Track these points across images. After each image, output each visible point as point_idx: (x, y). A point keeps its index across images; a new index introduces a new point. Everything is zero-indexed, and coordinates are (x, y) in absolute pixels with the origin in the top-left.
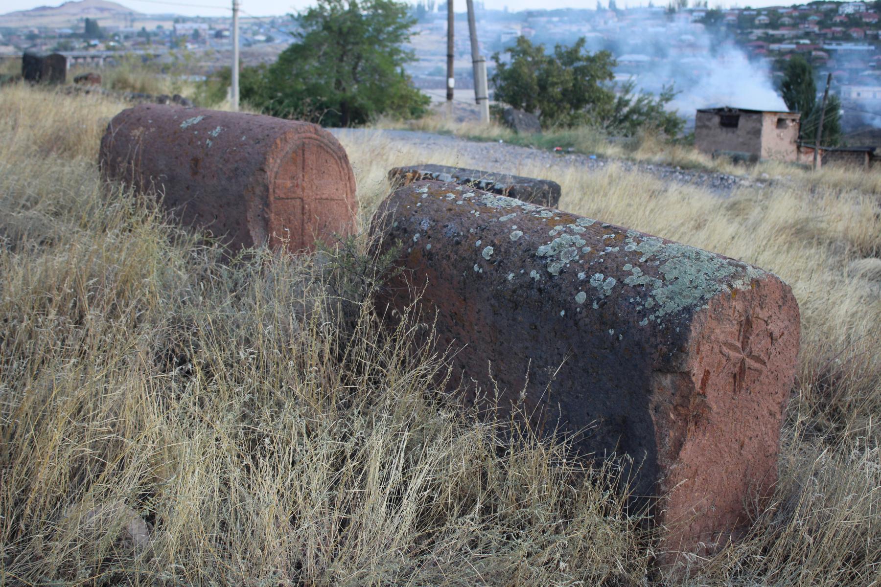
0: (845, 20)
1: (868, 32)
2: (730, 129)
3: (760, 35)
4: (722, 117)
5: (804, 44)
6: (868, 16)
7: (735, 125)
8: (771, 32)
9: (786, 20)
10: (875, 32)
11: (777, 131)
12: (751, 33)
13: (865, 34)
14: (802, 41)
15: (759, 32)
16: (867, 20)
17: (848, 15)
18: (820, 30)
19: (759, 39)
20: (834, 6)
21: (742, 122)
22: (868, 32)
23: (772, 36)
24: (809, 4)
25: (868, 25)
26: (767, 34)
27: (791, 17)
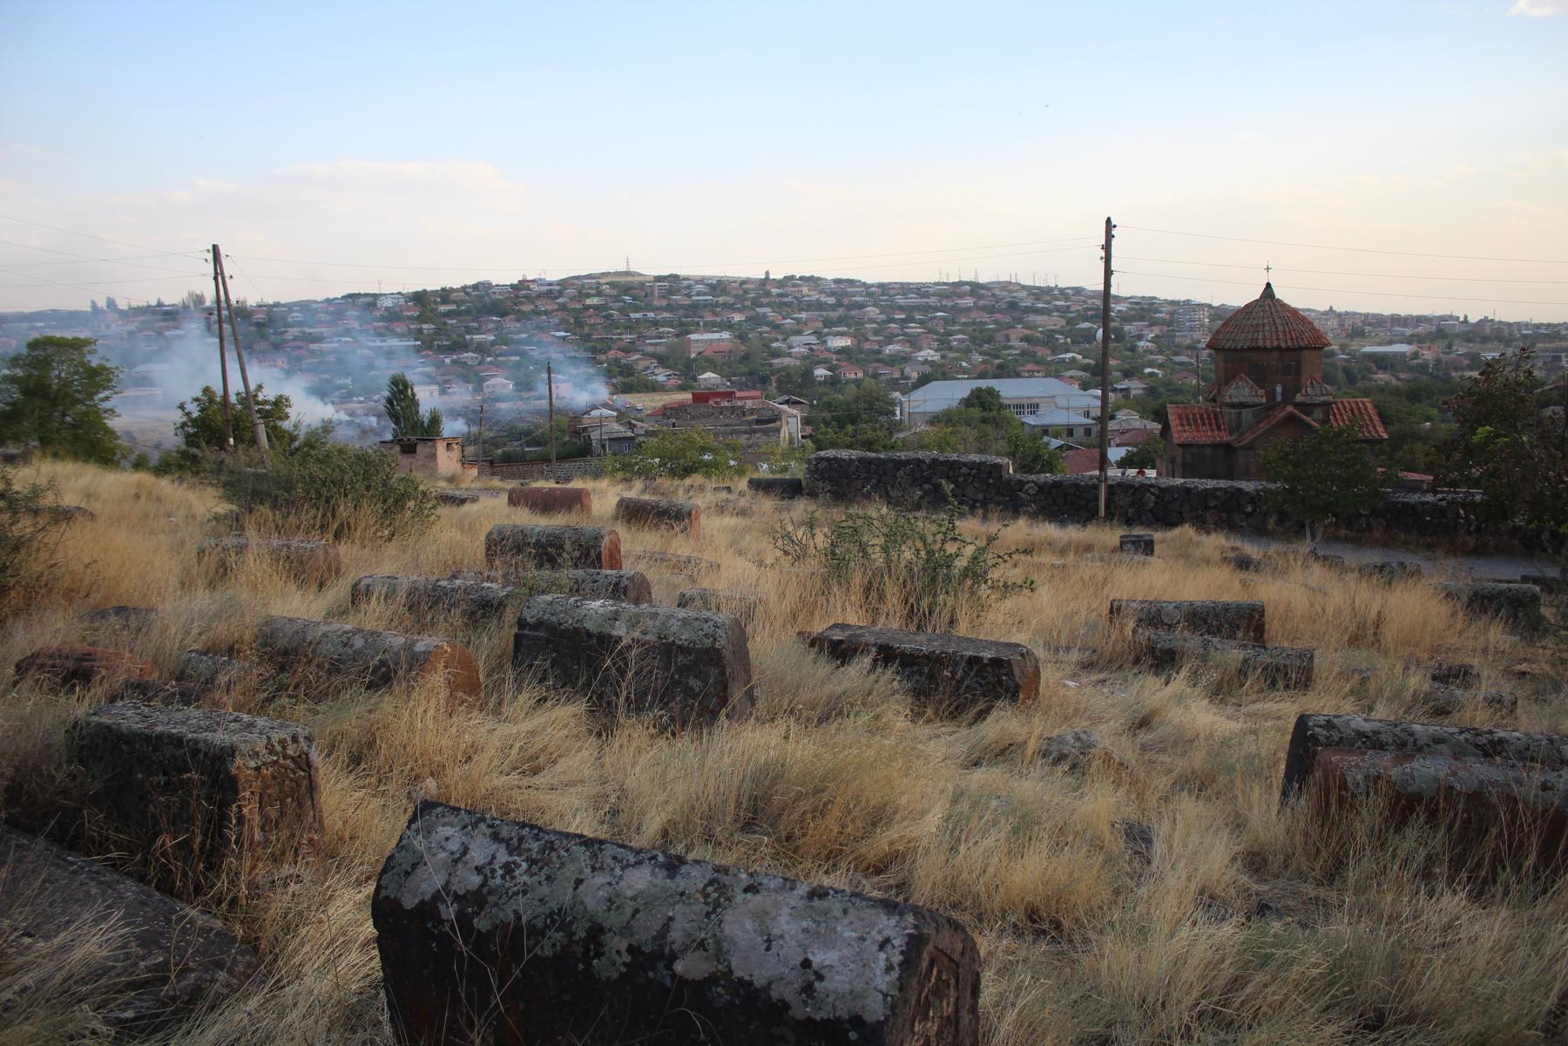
0: (386, 314)
1: (411, 326)
2: (410, 455)
3: (295, 334)
4: (402, 446)
5: (346, 342)
6: (409, 309)
7: (415, 452)
8: (308, 330)
9: (323, 317)
10: (418, 326)
11: (447, 453)
12: (286, 332)
13: (409, 329)
14: (344, 339)
15: (294, 331)
16: (409, 314)
17: (387, 309)
18: (361, 326)
19: (295, 339)
20: (370, 299)
21: (419, 448)
22: (411, 326)
23: (310, 334)
24: (343, 297)
25: (410, 318)
26: (304, 333)
27: (327, 312)
